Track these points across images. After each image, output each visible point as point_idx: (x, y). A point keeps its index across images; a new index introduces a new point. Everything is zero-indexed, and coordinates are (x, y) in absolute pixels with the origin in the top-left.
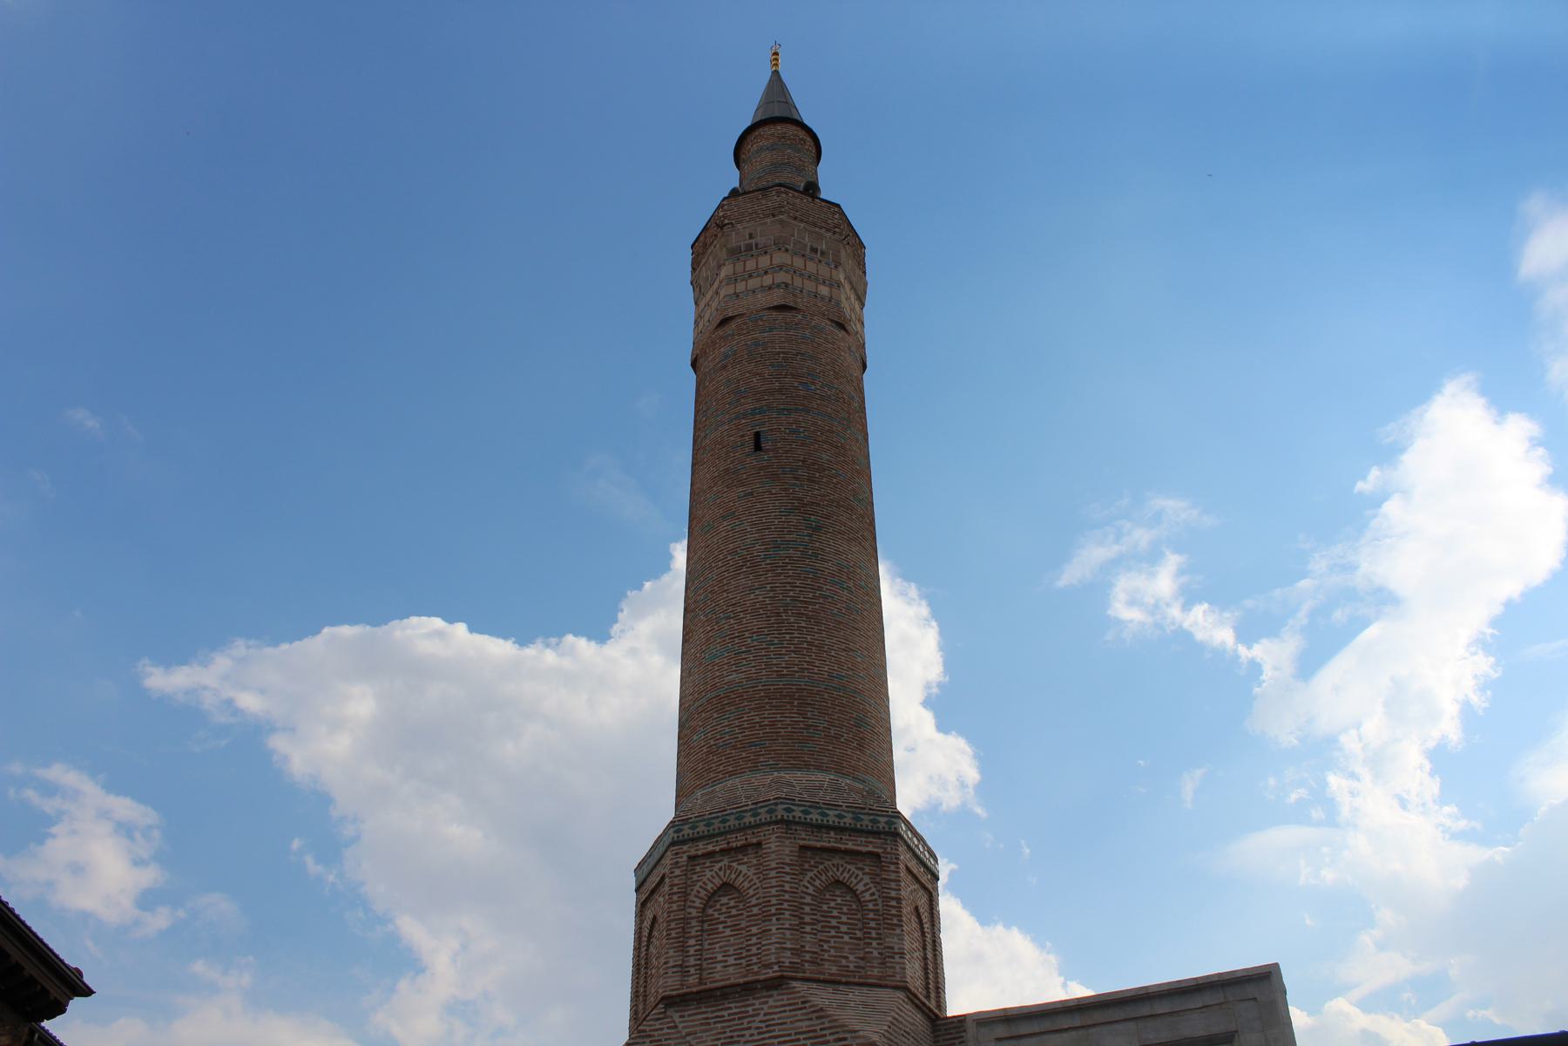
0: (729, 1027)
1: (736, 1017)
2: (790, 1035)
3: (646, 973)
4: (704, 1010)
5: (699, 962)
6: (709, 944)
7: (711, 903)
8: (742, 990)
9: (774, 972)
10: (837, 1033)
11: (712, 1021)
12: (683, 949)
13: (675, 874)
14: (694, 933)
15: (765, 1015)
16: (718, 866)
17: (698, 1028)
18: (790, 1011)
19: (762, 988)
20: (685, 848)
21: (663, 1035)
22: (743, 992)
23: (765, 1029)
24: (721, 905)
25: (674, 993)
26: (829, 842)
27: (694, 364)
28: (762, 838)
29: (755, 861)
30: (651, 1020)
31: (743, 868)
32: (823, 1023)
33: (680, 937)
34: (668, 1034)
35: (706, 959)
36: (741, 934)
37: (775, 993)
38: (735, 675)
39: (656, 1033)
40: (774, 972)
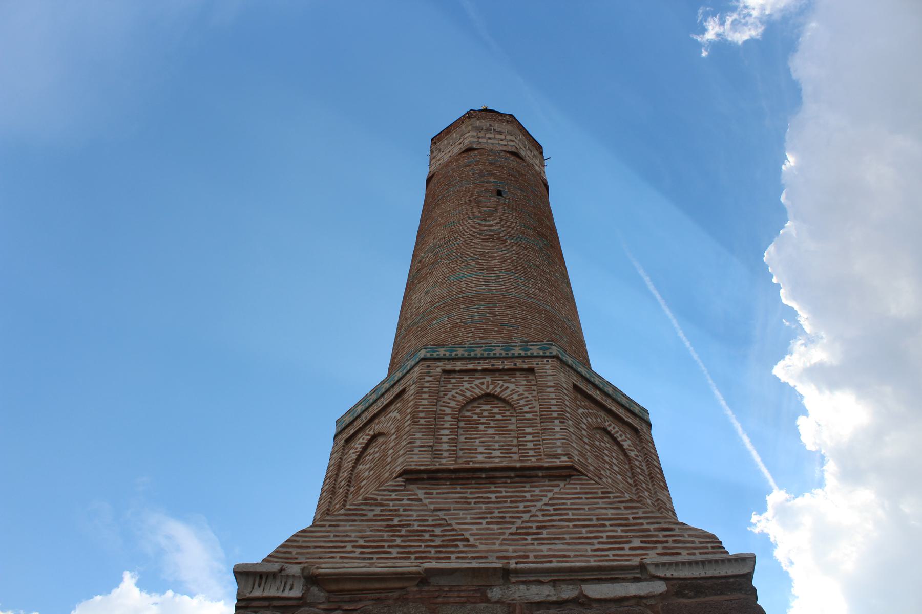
0: (498, 508)
1: (509, 500)
2: (591, 520)
3: (348, 490)
4: (459, 490)
5: (455, 448)
6: (466, 438)
7: (469, 408)
9: (561, 461)
10: (660, 523)
11: (473, 501)
12: (433, 430)
13: (425, 380)
14: (447, 425)
15: (550, 499)
16: (477, 382)
17: (452, 506)
18: (587, 498)
19: (543, 477)
20: (439, 364)
21: (402, 505)
22: (517, 479)
23: (552, 512)
24: (481, 410)
25: (422, 468)
26: (597, 396)
27: (429, 180)
28: (535, 366)
29: (525, 382)
30: (385, 490)
31: (512, 386)
32: (637, 513)
33: (432, 425)
34: (409, 505)
35: (461, 450)
36: (510, 434)
37: (562, 484)
38: (484, 287)
39: (391, 503)
40: (561, 461)
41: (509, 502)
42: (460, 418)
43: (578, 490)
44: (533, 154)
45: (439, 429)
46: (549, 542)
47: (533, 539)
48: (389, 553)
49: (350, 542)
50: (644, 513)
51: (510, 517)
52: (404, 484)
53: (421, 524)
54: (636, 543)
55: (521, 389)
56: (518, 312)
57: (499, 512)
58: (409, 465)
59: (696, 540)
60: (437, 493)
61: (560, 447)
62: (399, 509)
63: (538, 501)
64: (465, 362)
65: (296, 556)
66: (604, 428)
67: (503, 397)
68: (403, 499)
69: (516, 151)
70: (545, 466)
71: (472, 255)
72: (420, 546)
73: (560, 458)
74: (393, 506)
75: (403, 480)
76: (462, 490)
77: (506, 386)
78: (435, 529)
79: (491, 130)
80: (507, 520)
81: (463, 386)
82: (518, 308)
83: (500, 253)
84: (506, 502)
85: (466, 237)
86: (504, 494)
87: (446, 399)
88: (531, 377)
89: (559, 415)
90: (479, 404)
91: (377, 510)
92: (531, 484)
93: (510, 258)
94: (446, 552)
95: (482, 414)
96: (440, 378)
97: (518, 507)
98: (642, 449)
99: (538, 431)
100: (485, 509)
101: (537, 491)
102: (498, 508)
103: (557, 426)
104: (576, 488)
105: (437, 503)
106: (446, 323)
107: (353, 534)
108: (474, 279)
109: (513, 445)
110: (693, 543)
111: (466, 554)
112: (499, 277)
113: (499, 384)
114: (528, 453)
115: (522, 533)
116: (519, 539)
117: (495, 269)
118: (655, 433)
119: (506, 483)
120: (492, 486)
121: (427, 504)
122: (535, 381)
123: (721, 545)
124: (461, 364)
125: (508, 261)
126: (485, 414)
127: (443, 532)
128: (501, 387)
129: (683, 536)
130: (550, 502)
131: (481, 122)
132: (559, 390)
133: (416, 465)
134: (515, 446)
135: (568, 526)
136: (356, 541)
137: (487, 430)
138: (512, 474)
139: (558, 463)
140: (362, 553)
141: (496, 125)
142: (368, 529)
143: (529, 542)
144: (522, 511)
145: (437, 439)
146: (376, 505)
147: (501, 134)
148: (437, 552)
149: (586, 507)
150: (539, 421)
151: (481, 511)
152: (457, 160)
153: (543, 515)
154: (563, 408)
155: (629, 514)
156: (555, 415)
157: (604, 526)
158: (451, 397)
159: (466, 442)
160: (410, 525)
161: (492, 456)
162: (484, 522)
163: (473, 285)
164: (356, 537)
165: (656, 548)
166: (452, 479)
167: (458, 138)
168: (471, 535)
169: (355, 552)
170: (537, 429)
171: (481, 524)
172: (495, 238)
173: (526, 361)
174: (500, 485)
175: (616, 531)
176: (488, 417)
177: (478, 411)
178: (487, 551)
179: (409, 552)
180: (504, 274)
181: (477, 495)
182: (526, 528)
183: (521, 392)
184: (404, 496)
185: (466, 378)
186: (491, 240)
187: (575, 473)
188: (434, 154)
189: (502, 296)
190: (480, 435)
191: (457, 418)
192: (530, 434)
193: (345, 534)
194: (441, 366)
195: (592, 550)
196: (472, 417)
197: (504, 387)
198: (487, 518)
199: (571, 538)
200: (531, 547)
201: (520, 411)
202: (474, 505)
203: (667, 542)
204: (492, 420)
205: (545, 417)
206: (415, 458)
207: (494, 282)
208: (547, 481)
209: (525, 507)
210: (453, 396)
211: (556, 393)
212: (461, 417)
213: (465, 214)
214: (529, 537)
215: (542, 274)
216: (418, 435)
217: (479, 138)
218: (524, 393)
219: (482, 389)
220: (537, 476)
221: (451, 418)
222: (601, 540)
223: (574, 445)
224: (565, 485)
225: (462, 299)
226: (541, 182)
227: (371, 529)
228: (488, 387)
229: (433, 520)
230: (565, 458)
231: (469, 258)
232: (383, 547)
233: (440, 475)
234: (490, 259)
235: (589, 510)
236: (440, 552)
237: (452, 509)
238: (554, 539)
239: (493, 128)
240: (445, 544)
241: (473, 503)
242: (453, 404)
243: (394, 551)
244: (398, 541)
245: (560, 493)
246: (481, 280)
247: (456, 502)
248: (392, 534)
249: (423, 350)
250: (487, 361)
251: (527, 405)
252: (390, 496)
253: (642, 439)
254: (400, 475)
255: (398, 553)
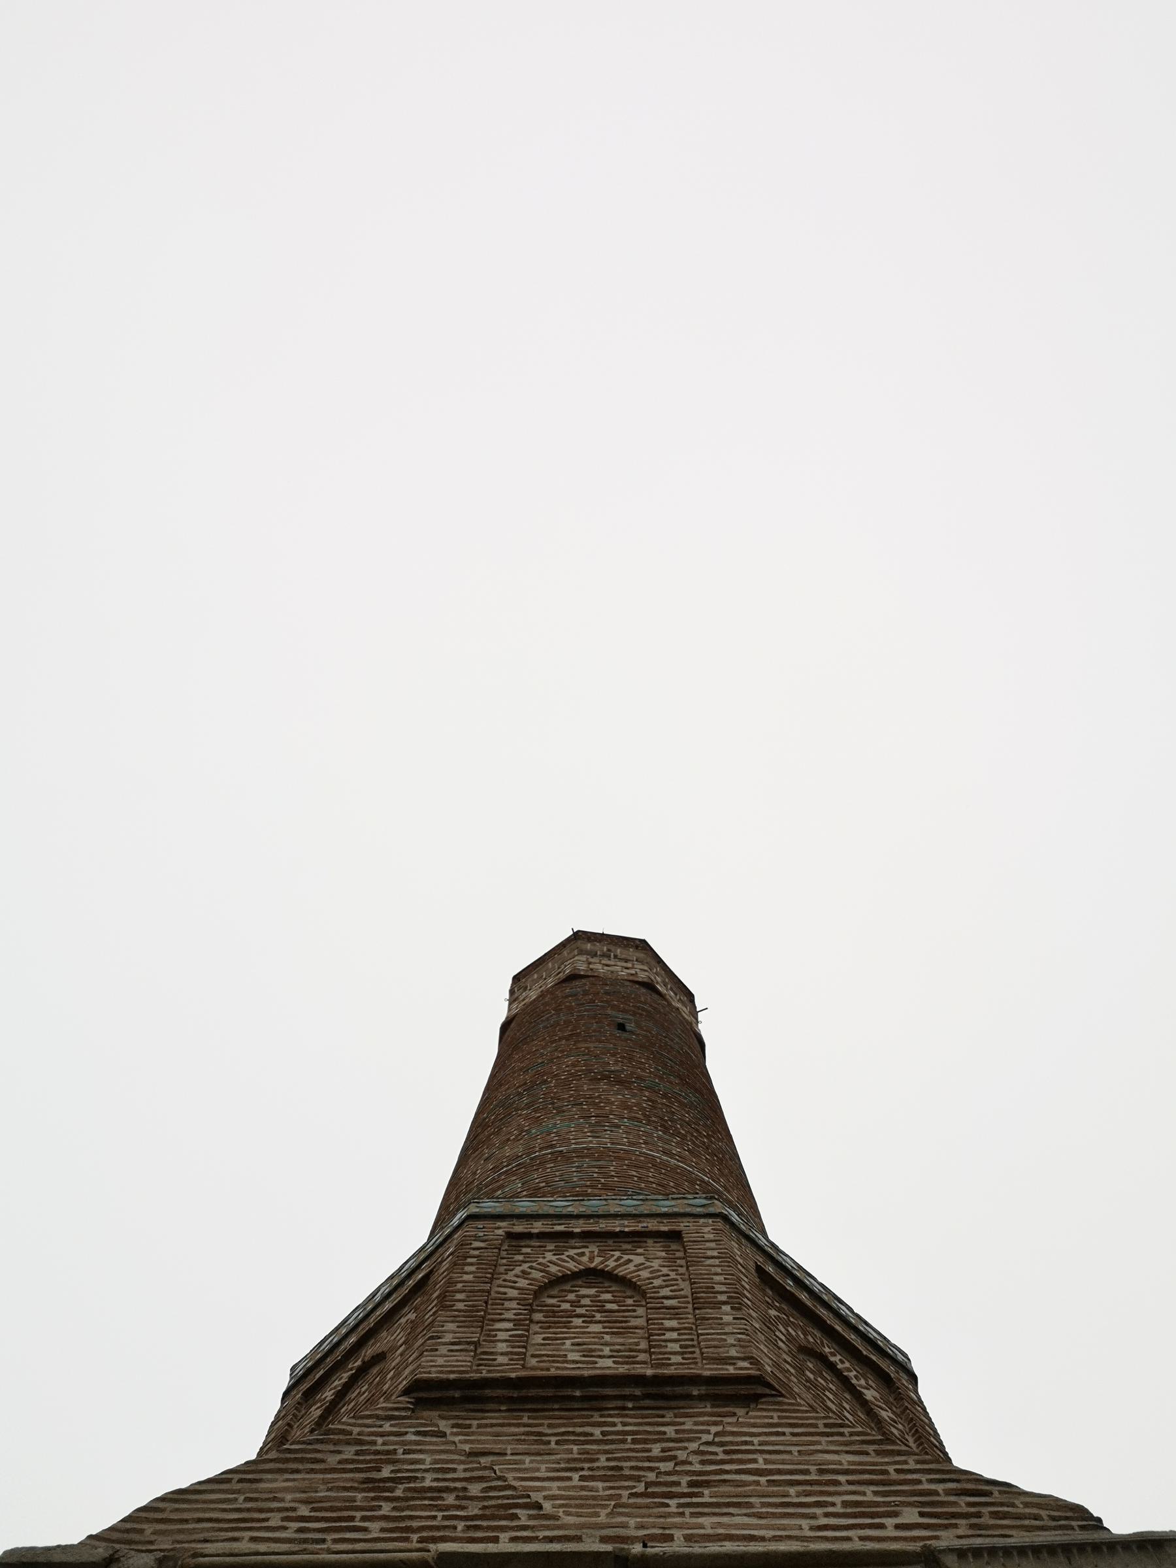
0: (606, 1452)
1: (629, 1438)
2: (807, 1472)
4: (525, 1420)
7: (555, 1292)
8: (647, 1396)
11: (553, 1439)
14: (509, 1315)
15: (717, 1434)
16: (572, 1252)
19: (701, 1398)
21: (403, 1443)
22: (647, 1403)
23: (721, 1456)
31: (638, 1260)
35: (533, 1356)
36: (635, 1333)
37: (741, 1412)
41: (629, 1441)
42: (535, 1308)
43: (776, 1420)
44: (678, 998)
45: (494, 1320)
46: (717, 1510)
47: (680, 1506)
48: (365, 1529)
49: (279, 1510)
50: (918, 1462)
51: (632, 1468)
52: (412, 1407)
53: (440, 1476)
54: (910, 1516)
55: (656, 1264)
56: (650, 1174)
57: (608, 1460)
58: (425, 1373)
59: (1043, 1513)
60: (479, 1426)
61: (734, 1346)
62: (395, 1450)
63: (689, 1440)
64: (550, 1223)
65: (153, 1538)
66: (821, 1353)
67: (621, 1274)
68: (406, 1433)
69: (650, 982)
70: (703, 1375)
71: (572, 1099)
72: (435, 1517)
73: (734, 1364)
74: (384, 1444)
75: (412, 1400)
76: (531, 1421)
77: (627, 1259)
78: (469, 1487)
79: (610, 956)
80: (627, 1472)
81: (544, 1258)
82: (652, 1170)
83: (619, 1097)
84: (624, 1441)
85: (563, 1077)
86: (619, 1428)
87: (510, 1276)
88: (674, 1246)
89: (729, 1297)
90: (572, 1287)
91: (349, 1452)
92: (676, 1411)
93: (638, 1104)
94: (489, 1528)
95: (579, 1301)
96: (501, 1244)
97: (649, 1450)
98: (903, 1412)
99: (690, 1325)
100: (580, 1454)
101: (689, 1424)
102: (606, 1452)
103: (727, 1314)
104: (772, 1417)
105: (479, 1442)
106: (519, 1190)
107: (289, 1497)
108: (572, 1129)
109: (639, 1351)
110: (1036, 1519)
111: (534, 1532)
112: (618, 1126)
113: (613, 1255)
114: (669, 1359)
115: (660, 1493)
116: (652, 1505)
117: (611, 1116)
118: (926, 1391)
119: (624, 1408)
120: (596, 1414)
121: (457, 1442)
122: (685, 1269)
123: (1100, 1525)
124: (543, 1224)
125: (635, 1108)
126: (586, 1301)
127: (486, 1492)
128: (616, 1261)
129: (1013, 1505)
130: (717, 1440)
131: (595, 945)
132: (729, 1262)
133: (441, 1372)
134: (645, 1351)
135: (757, 1483)
136: (294, 1509)
137: (588, 1327)
138: (638, 1392)
139: (731, 1370)
140: (300, 1530)
141: (619, 950)
142: (322, 1487)
143: (673, 1509)
144: (657, 1457)
145: (489, 1335)
146: (348, 1443)
147: (626, 962)
148: (468, 1528)
149: (795, 1449)
150: (690, 1309)
151: (570, 1456)
152: (552, 993)
153: (703, 1462)
154: (737, 1288)
155: (887, 1463)
156: (723, 1298)
157: (837, 1483)
158: (520, 1274)
159: (543, 1345)
160: (417, 1478)
161: (597, 1365)
162: (576, 1476)
163: (572, 1137)
164: (293, 1501)
165: (955, 1526)
166: (511, 1400)
167: (557, 967)
168: (545, 1498)
169: (286, 1528)
170: (689, 1323)
171: (570, 1479)
172: (612, 1079)
173: (665, 1221)
174: (612, 1412)
175: (864, 1494)
176: (591, 1307)
177: (571, 1297)
178: (582, 1526)
179: (409, 1529)
180: (627, 1124)
181: (563, 1430)
182: (666, 1484)
183: (656, 1268)
184: (409, 1427)
185: (551, 1246)
186: (605, 1081)
187: (768, 1391)
188: (516, 995)
189: (622, 1152)
190: (574, 1333)
191: (531, 1305)
192: (673, 1330)
193: (271, 1496)
194: (505, 1228)
195: (812, 1528)
196: (559, 1306)
197: (622, 1261)
198: (582, 1469)
199: (763, 1505)
200: (678, 1520)
201: (652, 1295)
202: (556, 1447)
203: (978, 1515)
204: (598, 1311)
205: (702, 1300)
206: (440, 1361)
207: (609, 1132)
208: (708, 1406)
209: (663, 1450)
210: (523, 1272)
211: (722, 1266)
212: (537, 1306)
213: (562, 1051)
214: (672, 1502)
215: (695, 1134)
216: (451, 1326)
217: (590, 963)
218: (662, 1269)
219: (580, 1263)
220: (689, 1397)
221: (518, 1304)
222: (830, 1509)
223: (762, 1347)
224: (747, 1413)
225: (550, 1156)
226: (692, 1033)
227: (330, 1485)
228: (591, 1259)
229: (465, 1470)
230: (746, 1364)
231: (566, 1104)
232: (352, 1519)
233: (488, 1392)
234: (602, 1105)
235: (800, 1455)
236: (477, 1528)
237: (509, 1452)
238: (728, 1505)
239: (612, 954)
240: (488, 1512)
241: (553, 1443)
242: (522, 1283)
243: (375, 1527)
244: (386, 1509)
245: (737, 1424)
246: (586, 1130)
247: (518, 1440)
248: (372, 1495)
249: (472, 1204)
250: (592, 1221)
251: (667, 1286)
252: (381, 1426)
253: (900, 1393)
254: (406, 1392)
255: (383, 1530)
